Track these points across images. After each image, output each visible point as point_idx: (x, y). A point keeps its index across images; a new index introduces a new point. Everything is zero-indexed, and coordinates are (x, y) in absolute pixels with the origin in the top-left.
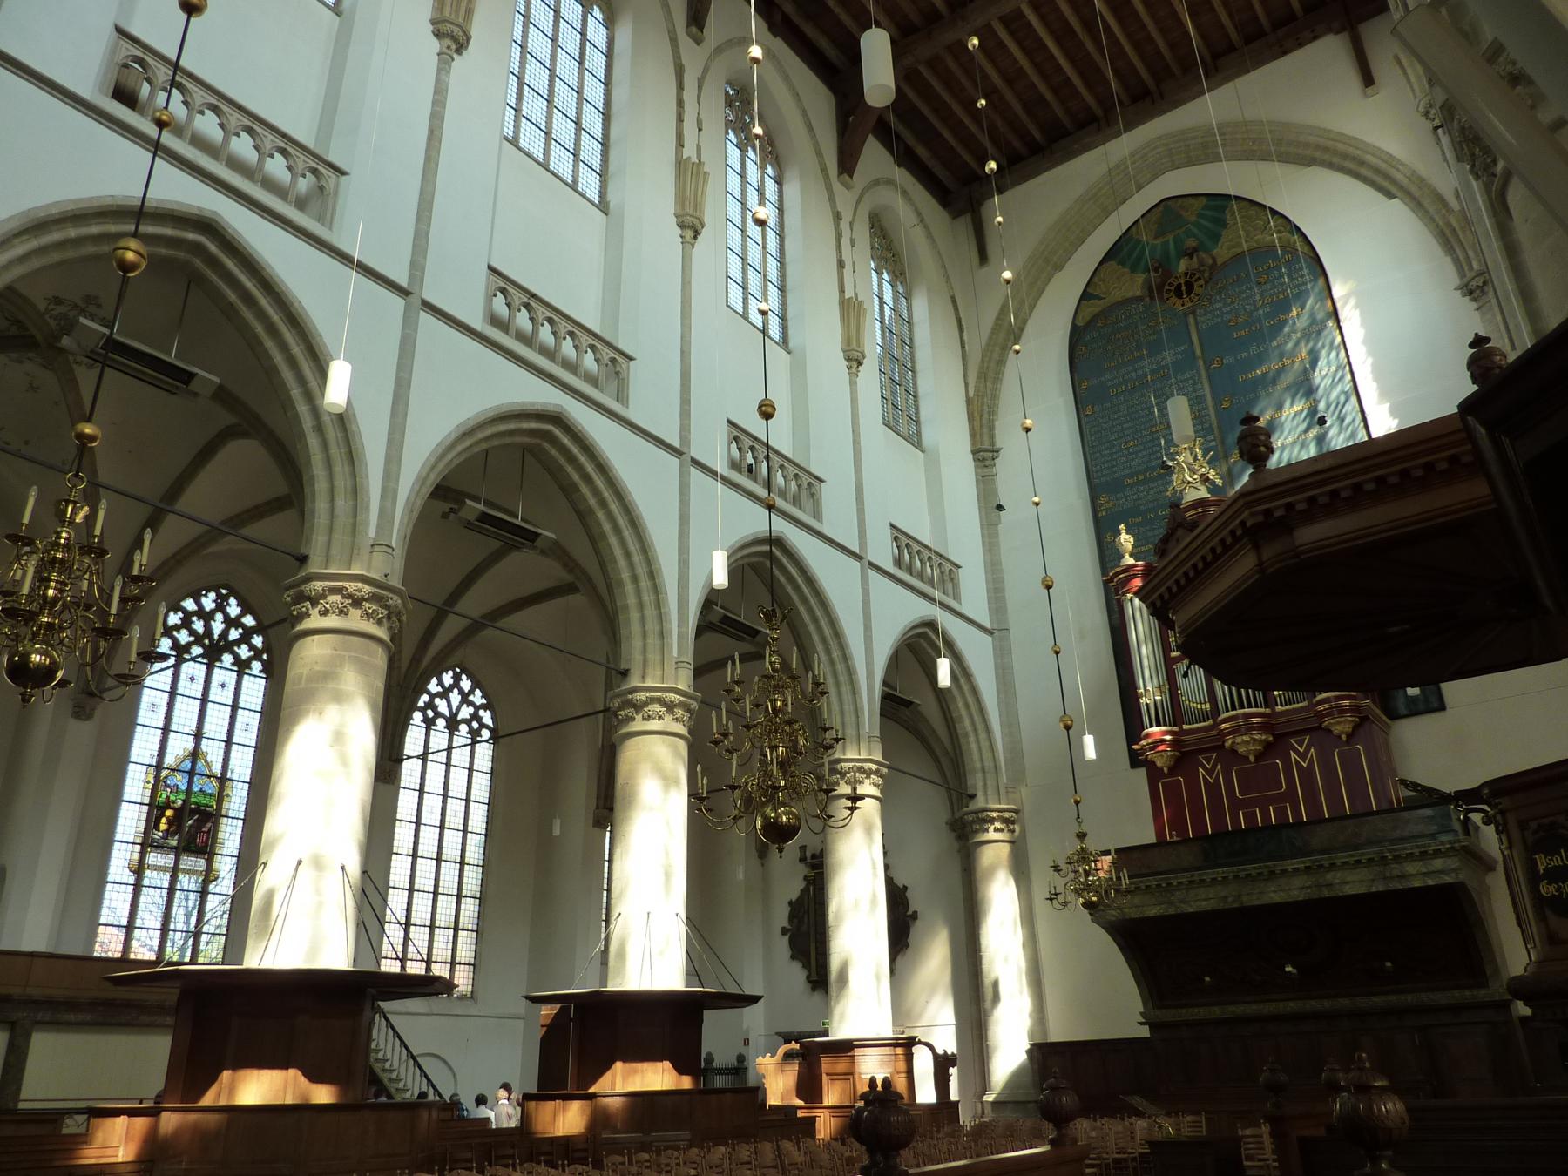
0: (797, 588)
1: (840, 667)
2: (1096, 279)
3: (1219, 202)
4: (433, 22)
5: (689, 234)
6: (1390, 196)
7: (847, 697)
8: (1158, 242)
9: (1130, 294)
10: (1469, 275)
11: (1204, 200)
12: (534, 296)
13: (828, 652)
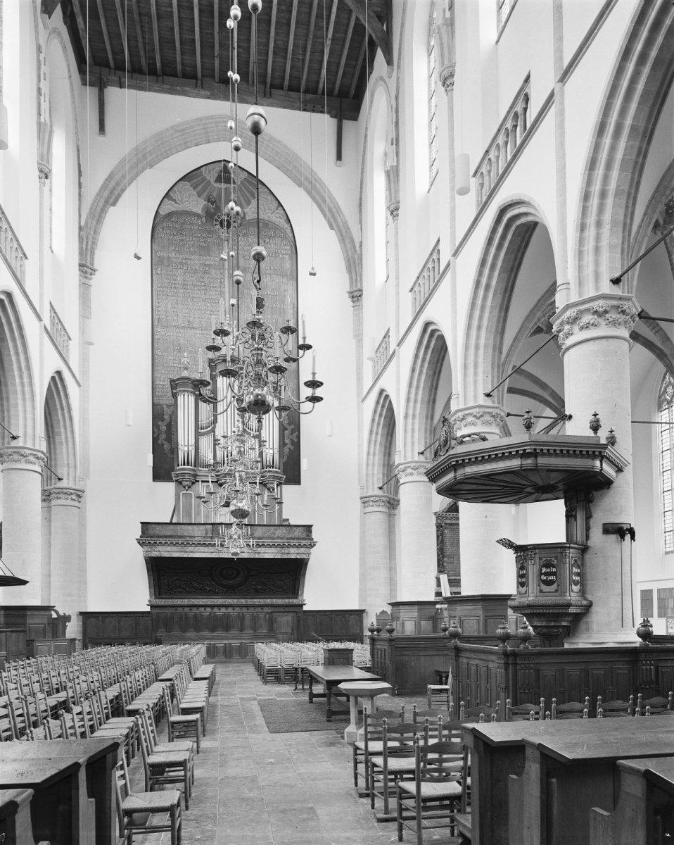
0: (11, 330)
1: (27, 389)
2: (175, 188)
3: (255, 183)
6: (332, 228)
7: (29, 409)
8: (217, 185)
9: (195, 210)
10: (354, 289)
11: (247, 174)
13: (21, 377)
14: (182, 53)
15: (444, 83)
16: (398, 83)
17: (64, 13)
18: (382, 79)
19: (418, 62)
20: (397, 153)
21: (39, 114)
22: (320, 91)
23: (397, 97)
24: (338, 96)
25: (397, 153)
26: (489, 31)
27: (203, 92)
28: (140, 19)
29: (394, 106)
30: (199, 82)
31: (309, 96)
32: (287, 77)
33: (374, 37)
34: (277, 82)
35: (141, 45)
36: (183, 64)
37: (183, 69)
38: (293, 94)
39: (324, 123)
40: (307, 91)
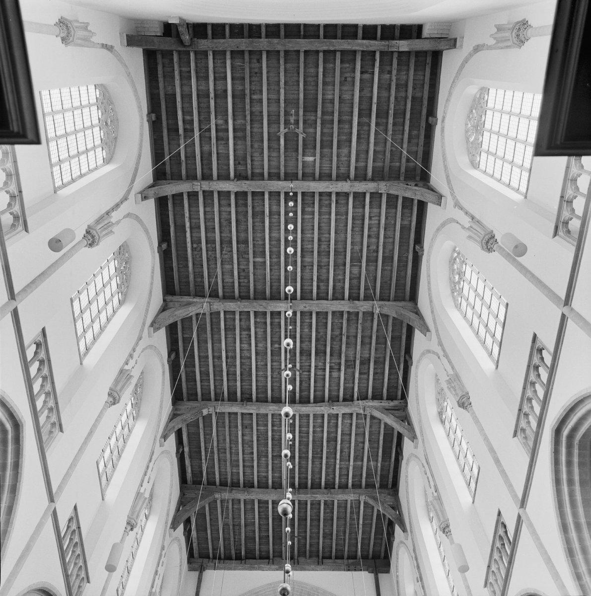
4: (111, 389)
5: (129, 528)
12: (79, 528)
14: (260, 544)
15: (444, 532)
16: (413, 542)
17: (185, 529)
18: (402, 542)
19: (424, 529)
20: (423, 587)
21: (152, 587)
22: (358, 557)
23: (414, 550)
24: (373, 558)
25: (423, 587)
26: (465, 497)
27: (273, 567)
28: (234, 529)
29: (414, 556)
30: (271, 561)
31: (351, 561)
32: (334, 550)
33: (391, 519)
34: (327, 554)
35: (232, 543)
36: (260, 551)
37: (260, 554)
38: (339, 561)
39: (363, 579)
40: (349, 558)
